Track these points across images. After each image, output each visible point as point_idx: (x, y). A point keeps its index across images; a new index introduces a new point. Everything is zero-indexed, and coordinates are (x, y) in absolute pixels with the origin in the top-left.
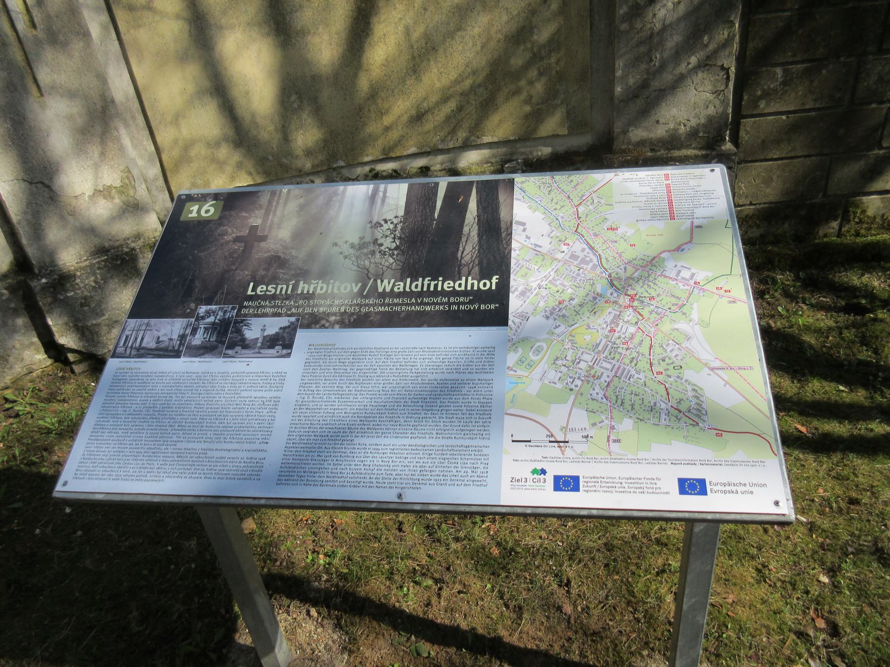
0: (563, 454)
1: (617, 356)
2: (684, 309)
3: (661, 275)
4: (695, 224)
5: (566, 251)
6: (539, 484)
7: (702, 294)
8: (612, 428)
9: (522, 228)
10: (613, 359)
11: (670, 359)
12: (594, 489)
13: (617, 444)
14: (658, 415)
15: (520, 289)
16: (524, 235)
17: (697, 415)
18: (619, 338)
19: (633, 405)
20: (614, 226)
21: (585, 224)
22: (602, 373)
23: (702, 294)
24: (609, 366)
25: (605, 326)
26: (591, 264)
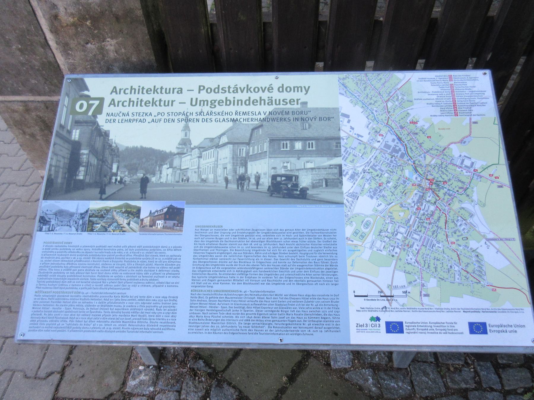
0: (391, 306)
1: (423, 229)
2: (469, 191)
3: (450, 163)
4: (473, 120)
5: (381, 141)
6: (376, 328)
7: (479, 180)
8: (423, 285)
9: (346, 120)
10: (420, 231)
11: (459, 231)
12: (413, 331)
13: (427, 298)
14: (453, 275)
15: (350, 173)
16: (349, 125)
17: (479, 275)
18: (424, 214)
19: (436, 268)
20: (415, 120)
21: (393, 117)
22: (414, 243)
23: (479, 180)
24: (417, 237)
25: (413, 205)
26: (400, 153)
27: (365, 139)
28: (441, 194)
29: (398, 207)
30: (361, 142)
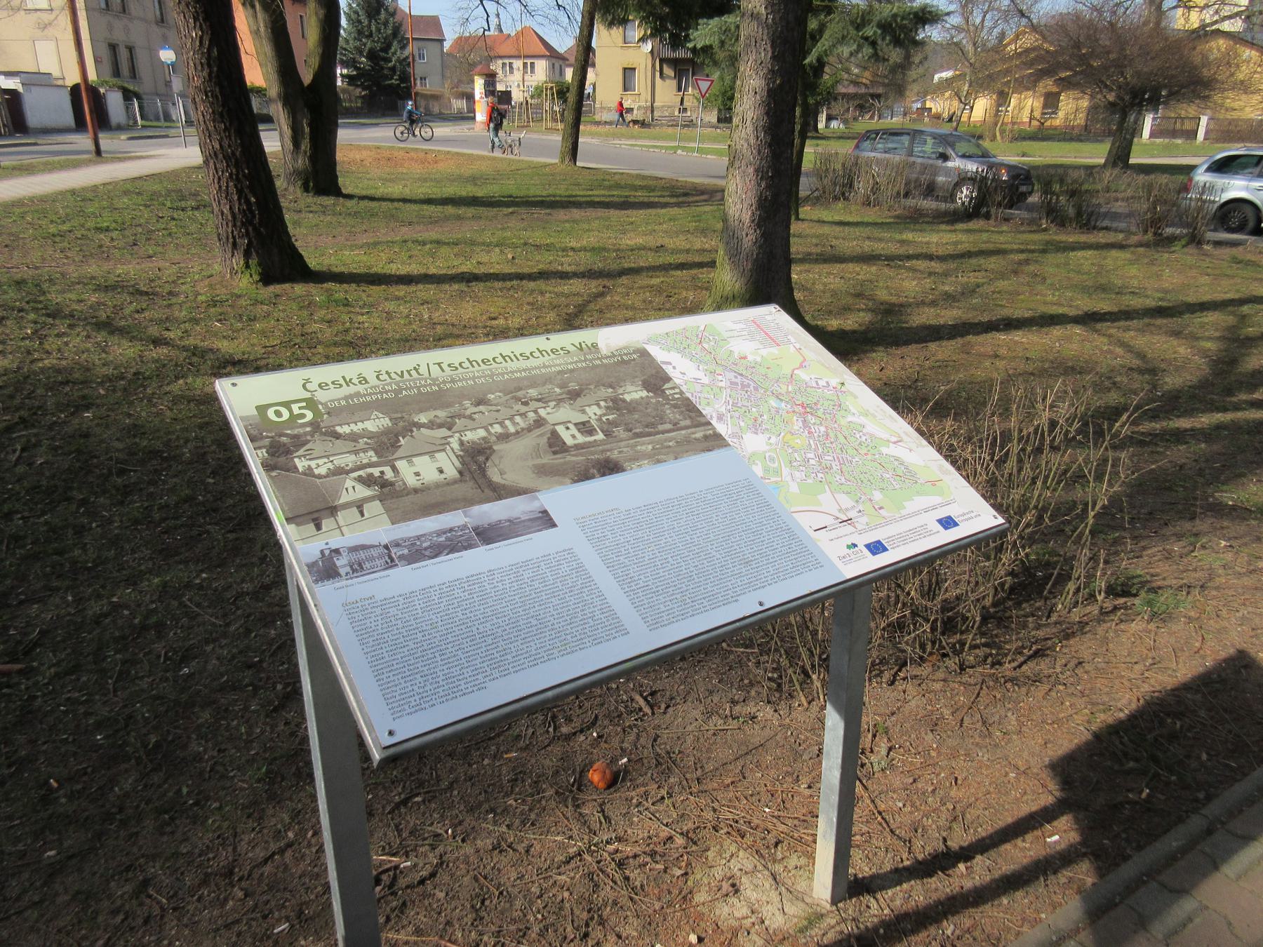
27: (706, 380)
28: (820, 413)
29: (789, 436)
30: (703, 385)
